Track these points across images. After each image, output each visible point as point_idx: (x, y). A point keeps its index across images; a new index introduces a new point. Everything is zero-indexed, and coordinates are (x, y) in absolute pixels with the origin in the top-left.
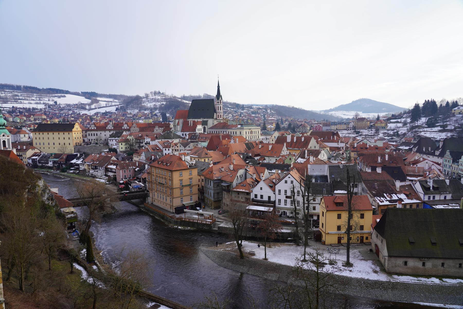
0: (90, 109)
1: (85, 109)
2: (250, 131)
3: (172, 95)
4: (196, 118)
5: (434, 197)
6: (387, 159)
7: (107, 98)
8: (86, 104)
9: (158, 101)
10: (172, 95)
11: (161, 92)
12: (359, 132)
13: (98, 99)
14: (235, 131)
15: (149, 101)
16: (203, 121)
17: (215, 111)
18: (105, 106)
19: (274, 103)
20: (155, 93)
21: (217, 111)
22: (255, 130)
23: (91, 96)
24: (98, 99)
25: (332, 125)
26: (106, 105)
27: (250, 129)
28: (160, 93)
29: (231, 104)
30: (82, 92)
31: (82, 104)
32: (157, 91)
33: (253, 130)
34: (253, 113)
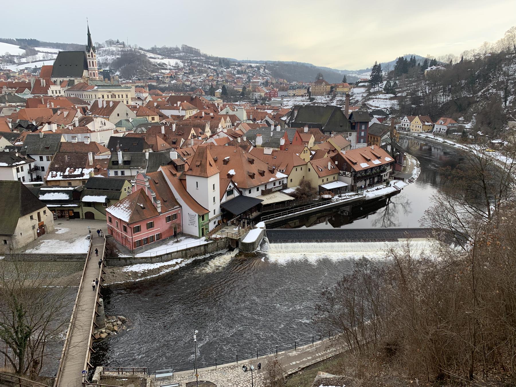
0: (20, 64)
1: (12, 62)
2: (110, 95)
3: (136, 45)
4: (61, 77)
5: (123, 173)
6: (174, 130)
7: (54, 48)
8: (14, 56)
9: (112, 53)
10: (136, 45)
11: (121, 41)
12: (314, 99)
13: (37, 49)
14: (90, 93)
15: (100, 54)
16: (70, 80)
17: (86, 68)
18: (42, 59)
19: (265, 59)
20: (111, 43)
21: (89, 67)
22: (120, 94)
23: (29, 45)
24: (37, 49)
25: (290, 89)
26: (44, 58)
27: (110, 92)
28: (118, 42)
29: (216, 59)
30: (17, 39)
31: (10, 56)
32: (115, 39)
33: (117, 94)
34: (239, 72)
